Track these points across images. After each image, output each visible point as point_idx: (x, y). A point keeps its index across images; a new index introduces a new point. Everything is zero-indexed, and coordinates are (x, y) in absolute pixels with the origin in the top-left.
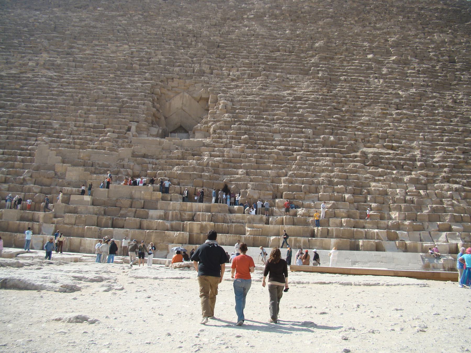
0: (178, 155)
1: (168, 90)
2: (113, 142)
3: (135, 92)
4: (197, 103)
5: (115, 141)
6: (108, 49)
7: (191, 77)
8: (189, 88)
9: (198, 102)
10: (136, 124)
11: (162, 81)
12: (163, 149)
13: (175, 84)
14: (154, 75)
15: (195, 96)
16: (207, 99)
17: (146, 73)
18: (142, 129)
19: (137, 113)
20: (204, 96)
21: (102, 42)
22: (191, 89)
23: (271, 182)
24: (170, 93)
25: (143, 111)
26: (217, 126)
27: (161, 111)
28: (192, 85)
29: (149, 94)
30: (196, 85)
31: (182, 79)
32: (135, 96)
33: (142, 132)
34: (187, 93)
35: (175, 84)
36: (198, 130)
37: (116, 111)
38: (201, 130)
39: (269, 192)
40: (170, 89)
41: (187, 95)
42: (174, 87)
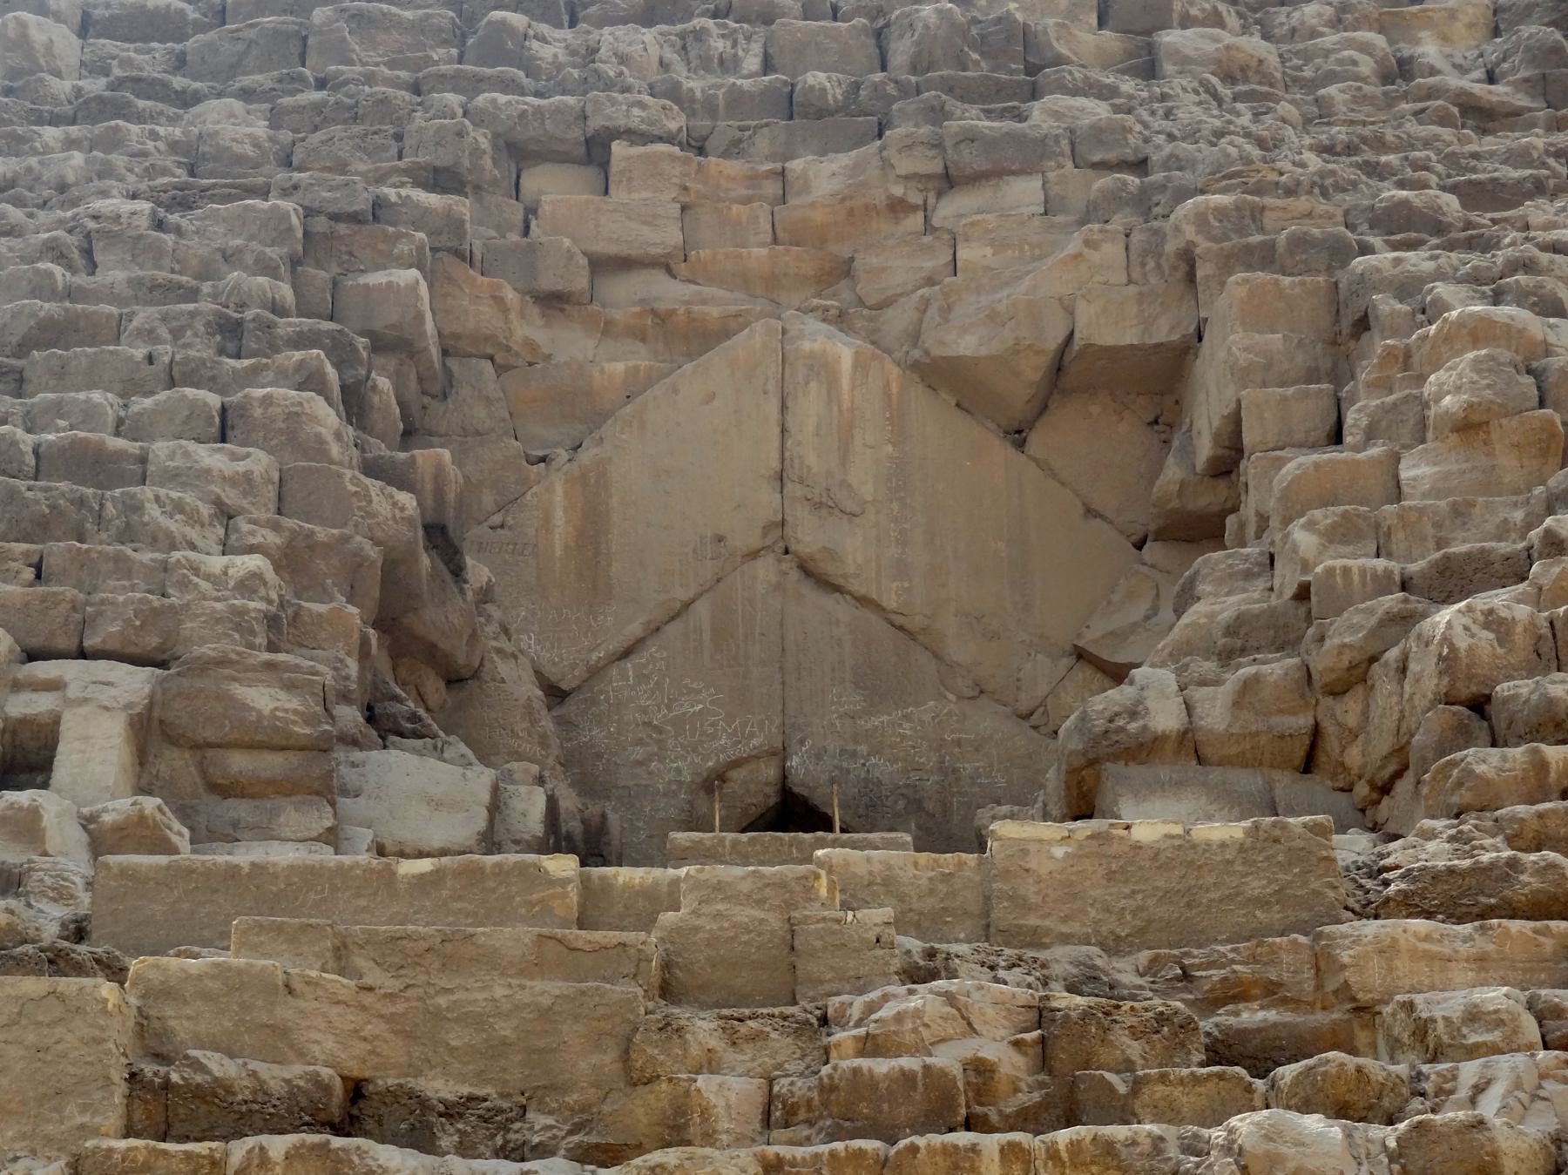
0: (980, 1069)
1: (553, 302)
3: (70, 294)
4: (1001, 450)
7: (860, 119)
8: (846, 269)
9: (1018, 436)
10: (134, 683)
11: (441, 179)
12: (667, 991)
13: (638, 208)
14: (319, 117)
15: (965, 342)
16: (1156, 381)
17: (188, 100)
18: (240, 763)
19: (127, 534)
20: (1115, 323)
22: (894, 264)
24: (570, 344)
25: (226, 515)
26: (1492, 621)
27: (478, 572)
28: (898, 207)
29: (278, 309)
30: (948, 210)
31: (734, 149)
32: (51, 334)
33: (240, 809)
34: (841, 320)
35: (638, 208)
36: (1145, 749)
38: (1191, 747)
40: (580, 282)
41: (844, 351)
42: (624, 264)
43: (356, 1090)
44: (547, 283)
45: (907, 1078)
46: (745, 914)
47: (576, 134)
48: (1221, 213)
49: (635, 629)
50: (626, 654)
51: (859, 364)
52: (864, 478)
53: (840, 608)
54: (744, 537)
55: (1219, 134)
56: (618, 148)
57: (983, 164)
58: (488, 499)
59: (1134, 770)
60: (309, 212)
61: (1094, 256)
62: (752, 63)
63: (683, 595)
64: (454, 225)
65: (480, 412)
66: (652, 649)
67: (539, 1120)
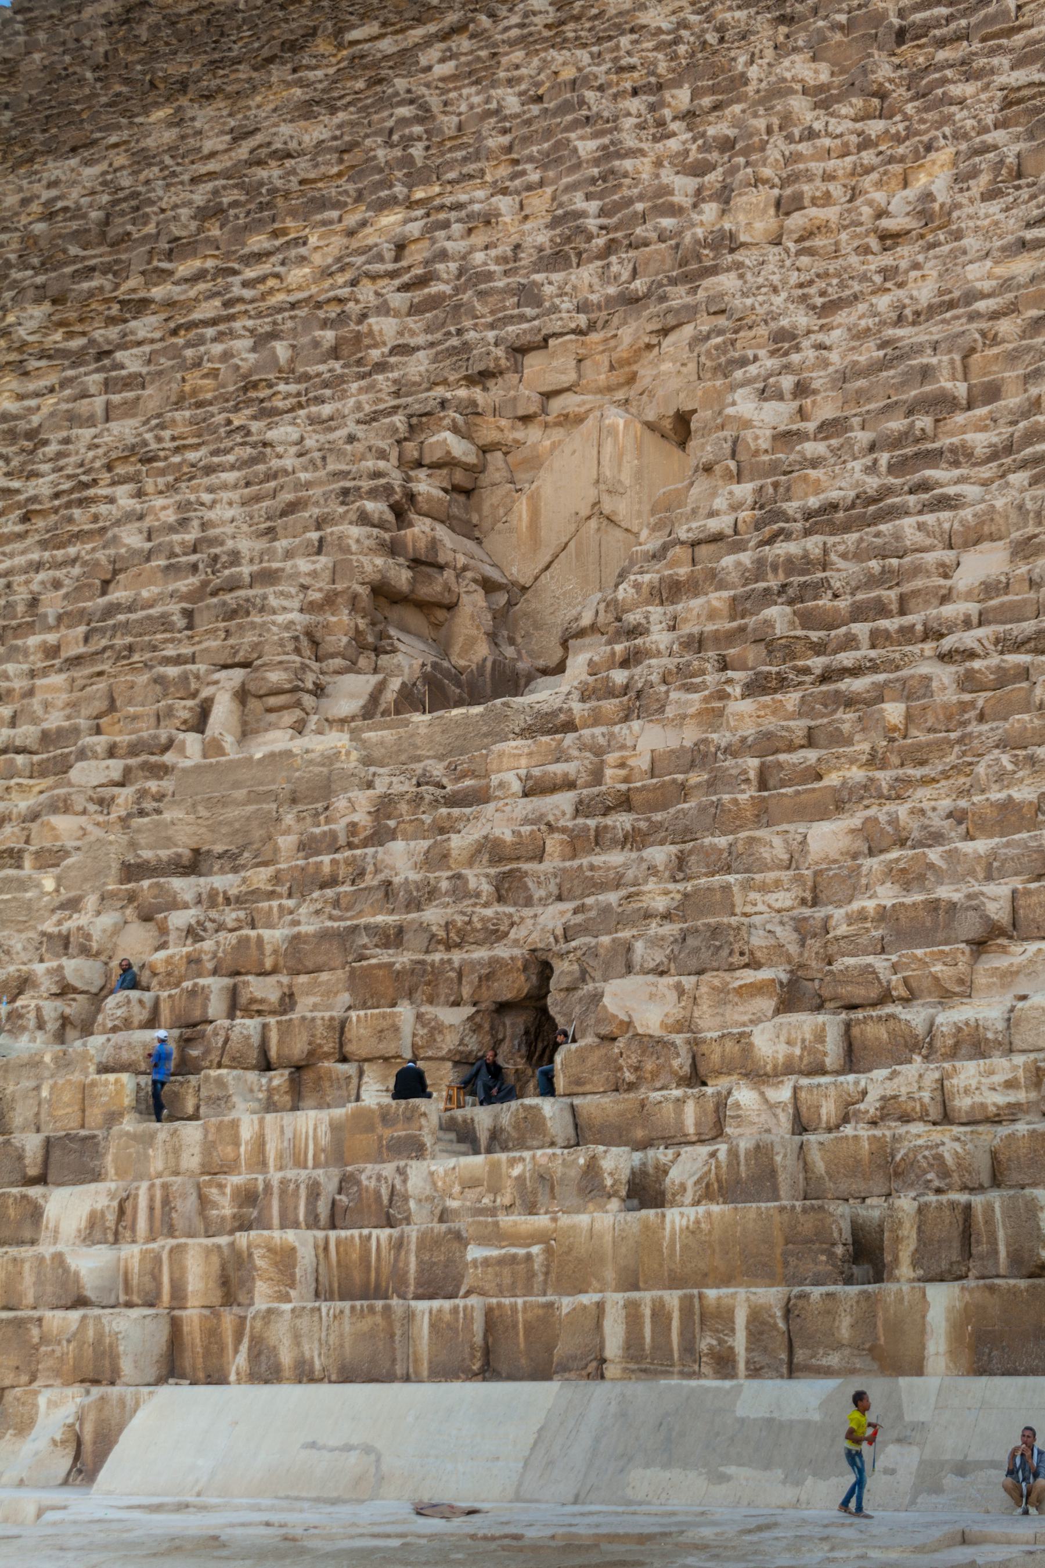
2: (84, 812)
5: (101, 802)
6: (303, 260)
21: (284, 232)
23: (803, 902)
24: (532, 434)
28: (649, 347)
33: (272, 717)
36: (581, 633)
37: (164, 623)
39: (749, 976)
40: (533, 409)
42: (557, 393)
43: (196, 852)
44: (521, 412)
45: (325, 833)
46: (317, 769)
47: (539, 338)
48: (717, 347)
49: (548, 558)
50: (547, 567)
51: (626, 425)
52: (626, 478)
53: (619, 534)
54: (585, 512)
55: (759, 288)
56: (552, 342)
57: (674, 323)
58: (501, 511)
59: (579, 641)
60: (410, 416)
61: (684, 370)
62: (625, 275)
63: (564, 540)
64: (474, 403)
65: (497, 477)
66: (555, 565)
67: (246, 855)
